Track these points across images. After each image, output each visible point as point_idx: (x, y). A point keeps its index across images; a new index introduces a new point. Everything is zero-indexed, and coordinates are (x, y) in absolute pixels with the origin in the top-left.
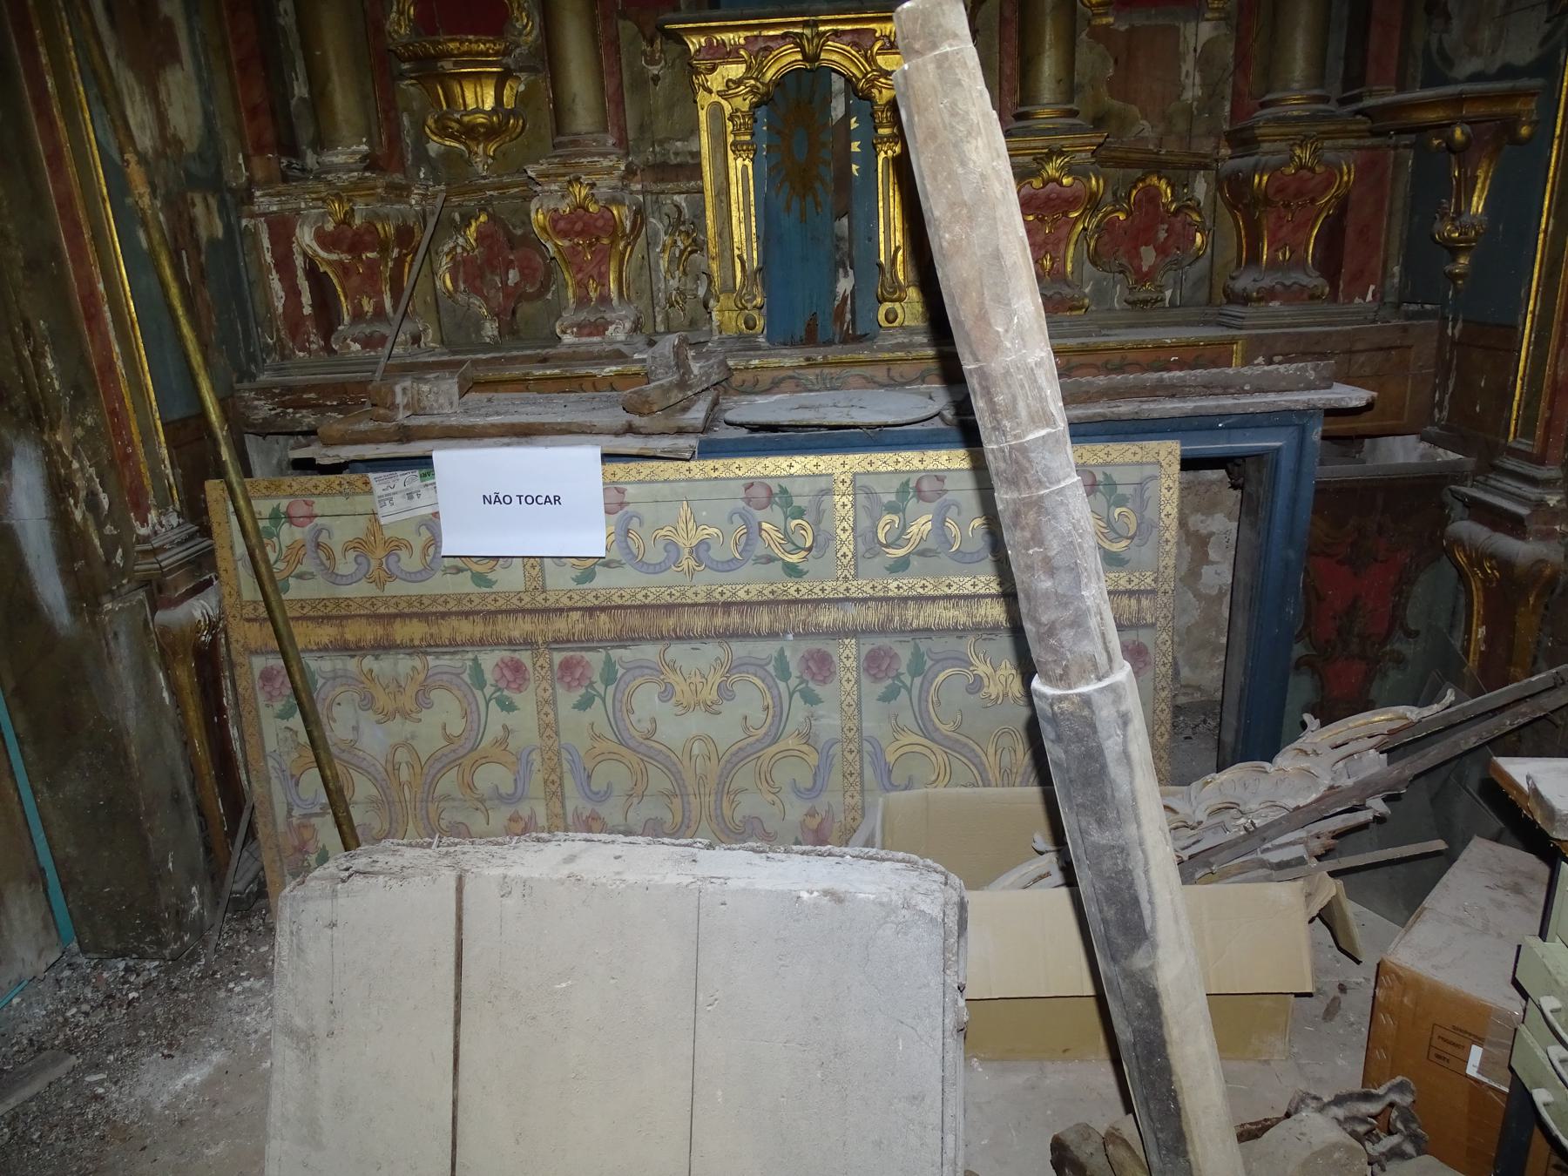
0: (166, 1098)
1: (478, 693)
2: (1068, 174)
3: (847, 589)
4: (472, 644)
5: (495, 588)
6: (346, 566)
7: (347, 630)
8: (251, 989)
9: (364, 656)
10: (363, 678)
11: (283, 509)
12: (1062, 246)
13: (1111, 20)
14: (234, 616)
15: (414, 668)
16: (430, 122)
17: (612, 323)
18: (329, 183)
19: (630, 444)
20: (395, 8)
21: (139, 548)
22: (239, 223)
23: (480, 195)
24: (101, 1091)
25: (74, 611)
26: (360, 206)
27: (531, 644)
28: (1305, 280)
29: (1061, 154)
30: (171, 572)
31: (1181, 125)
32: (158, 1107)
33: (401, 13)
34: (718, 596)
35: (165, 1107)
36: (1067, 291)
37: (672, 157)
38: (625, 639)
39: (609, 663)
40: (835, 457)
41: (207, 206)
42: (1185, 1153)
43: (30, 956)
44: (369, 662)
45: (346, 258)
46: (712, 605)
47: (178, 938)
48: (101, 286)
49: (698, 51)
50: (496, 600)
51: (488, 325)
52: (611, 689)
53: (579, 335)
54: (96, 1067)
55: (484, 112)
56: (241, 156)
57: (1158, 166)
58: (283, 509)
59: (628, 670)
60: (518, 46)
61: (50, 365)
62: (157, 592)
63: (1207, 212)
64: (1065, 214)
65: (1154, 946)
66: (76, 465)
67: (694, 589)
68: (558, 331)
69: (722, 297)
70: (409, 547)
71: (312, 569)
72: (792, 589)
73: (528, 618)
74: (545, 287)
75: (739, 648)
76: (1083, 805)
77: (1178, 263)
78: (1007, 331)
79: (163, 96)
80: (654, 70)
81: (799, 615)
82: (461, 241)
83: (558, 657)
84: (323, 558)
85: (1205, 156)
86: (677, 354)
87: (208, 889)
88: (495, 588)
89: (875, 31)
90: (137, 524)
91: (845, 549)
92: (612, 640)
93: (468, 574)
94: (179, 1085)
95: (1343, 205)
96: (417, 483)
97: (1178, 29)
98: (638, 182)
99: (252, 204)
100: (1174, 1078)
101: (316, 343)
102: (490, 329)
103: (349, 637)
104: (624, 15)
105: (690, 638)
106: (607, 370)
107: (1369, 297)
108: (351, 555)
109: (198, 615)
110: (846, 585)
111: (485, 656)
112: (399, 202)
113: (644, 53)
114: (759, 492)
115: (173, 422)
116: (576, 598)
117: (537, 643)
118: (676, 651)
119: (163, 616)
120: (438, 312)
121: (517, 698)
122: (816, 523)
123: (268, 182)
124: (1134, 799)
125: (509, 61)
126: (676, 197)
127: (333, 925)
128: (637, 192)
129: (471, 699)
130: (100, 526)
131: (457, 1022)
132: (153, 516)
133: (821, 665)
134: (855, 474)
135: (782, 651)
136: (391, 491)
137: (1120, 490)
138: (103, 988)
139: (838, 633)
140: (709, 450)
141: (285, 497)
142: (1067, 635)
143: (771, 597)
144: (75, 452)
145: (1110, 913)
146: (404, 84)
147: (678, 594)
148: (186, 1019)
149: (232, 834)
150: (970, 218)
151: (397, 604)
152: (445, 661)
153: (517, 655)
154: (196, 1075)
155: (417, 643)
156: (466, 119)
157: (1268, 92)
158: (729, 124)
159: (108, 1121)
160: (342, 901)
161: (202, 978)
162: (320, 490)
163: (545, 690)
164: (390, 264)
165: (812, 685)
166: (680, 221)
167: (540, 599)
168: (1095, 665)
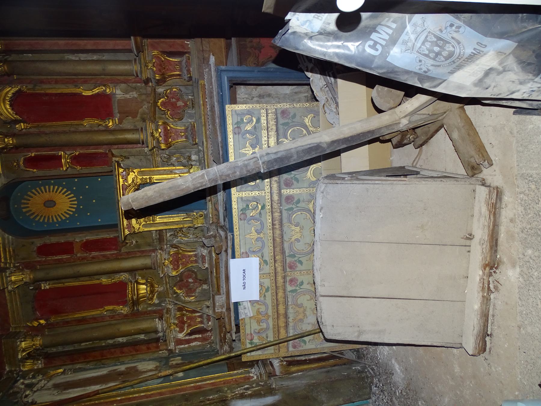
0: (401, 374)
1: (298, 291)
2: (158, 130)
3: (268, 192)
4: (285, 292)
5: (270, 286)
6: (264, 325)
7: (281, 326)
8: (379, 353)
9: (289, 321)
10: (295, 321)
11: (249, 341)
12: (177, 130)
13: (117, 119)
14: (278, 355)
15: (292, 308)
16: (150, 302)
17: (202, 254)
18: (166, 329)
19: (230, 251)
20: (121, 311)
21: (260, 379)
22: (177, 353)
23: (169, 289)
24: (400, 391)
25: (275, 395)
26: (172, 321)
27: (284, 277)
28: (184, 61)
29: (152, 133)
30: (266, 371)
31: (144, 97)
32: (403, 376)
33: (122, 310)
34: (270, 227)
35: (403, 374)
36: (189, 128)
37: (157, 237)
38: (283, 252)
39: (290, 256)
40: (232, 197)
41: (173, 361)
42: (373, 130)
44: (290, 320)
45: (186, 325)
46: (273, 229)
47: (366, 372)
48: (192, 385)
49: (129, 231)
50: (273, 286)
51: (204, 287)
52: (297, 255)
53: (205, 263)
54: (395, 393)
55: (147, 288)
56: (160, 352)
57: (156, 103)
58: (249, 341)
59: (291, 251)
60: (129, 279)
61: (211, 397)
62: (271, 375)
63: (167, 88)
64: (169, 130)
65: (321, 143)
66: (237, 392)
67: (269, 234)
68: (204, 268)
69: (194, 224)
70: (259, 309)
71: (265, 334)
72: (268, 207)
73: (277, 278)
74: (193, 272)
75: (285, 221)
76: (288, 161)
77: (182, 95)
78: (185, 185)
79: (145, 370)
80: (134, 242)
81: (275, 206)
82: (181, 294)
83: (288, 270)
84: (262, 331)
85: (152, 90)
86: (207, 238)
87: (354, 365)
88: (270, 286)
89: (122, 184)
90: (253, 379)
91: (257, 194)
92: (283, 255)
93: (266, 293)
94: (399, 371)
95: (164, 53)
96: (242, 306)
97: (118, 100)
98: (164, 246)
99: (172, 349)
100: (354, 135)
101: (209, 334)
102: (205, 287)
103: (283, 325)
104: (120, 250)
105: (282, 234)
106: (213, 255)
107: (188, 43)
108: (261, 324)
109: (278, 364)
110: (267, 193)
111: (288, 289)
112: (171, 311)
113: (130, 245)
114: (242, 217)
115: (228, 370)
116: (272, 265)
117: (284, 275)
118: (286, 238)
119: (278, 373)
120: (201, 301)
121: (299, 281)
122: (250, 201)
123: (166, 345)
124: (286, 150)
125: (133, 281)
126: (168, 236)
127: (333, 326)
128: (167, 246)
129: (300, 293)
130: (253, 387)
131: (355, 297)
132: (251, 375)
133: (289, 199)
134: (237, 191)
135: (285, 210)
136: (244, 313)
137: (239, 120)
138: (380, 393)
139: (280, 194)
140: (231, 230)
141: (246, 341)
142: (249, 168)
143: (270, 213)
144: (234, 393)
145: (314, 153)
146: (140, 309)
147: (270, 238)
148: (385, 370)
149: (340, 358)
150: (163, 194)
151: (274, 312)
152: (290, 300)
153: (288, 281)
154: (397, 367)
155: (285, 307)
156: (149, 293)
157: (134, 75)
158: (148, 222)
160: (327, 323)
161: (377, 366)
162: (244, 332)
163: (297, 273)
164: (187, 313)
165: (294, 201)
166: (174, 235)
167: (272, 275)
168: (255, 161)
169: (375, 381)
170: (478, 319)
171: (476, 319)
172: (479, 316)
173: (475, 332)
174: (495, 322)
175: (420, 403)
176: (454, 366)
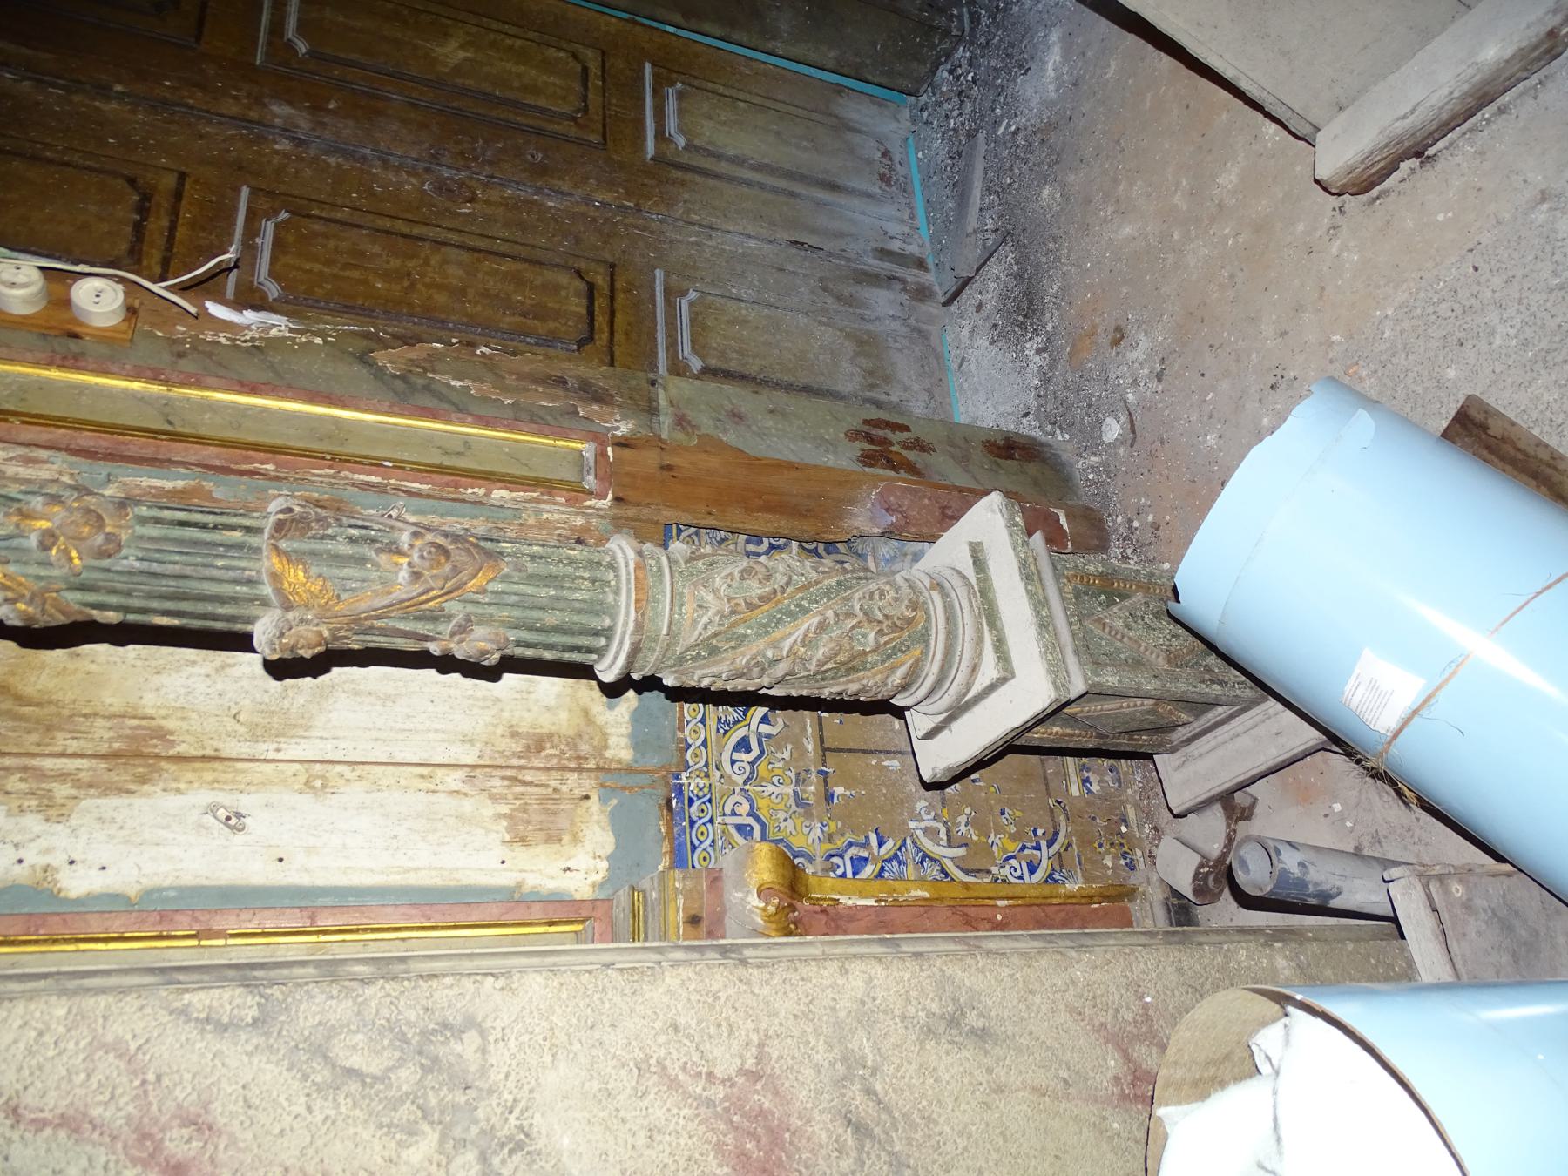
0: (1052, 87)
24: (1013, 128)
32: (1053, 95)
35: (1057, 90)
43: (893, 126)
54: (997, 123)
94: (1051, 73)
148: (1012, 45)
154: (1054, 57)
159: (1035, 133)
161: (994, 19)
169: (957, 56)
170: (1451, 93)
171: (1445, 91)
172: (1466, 87)
173: (1400, 127)
174: (1485, 133)
175: (1046, 192)
176: (1229, 165)
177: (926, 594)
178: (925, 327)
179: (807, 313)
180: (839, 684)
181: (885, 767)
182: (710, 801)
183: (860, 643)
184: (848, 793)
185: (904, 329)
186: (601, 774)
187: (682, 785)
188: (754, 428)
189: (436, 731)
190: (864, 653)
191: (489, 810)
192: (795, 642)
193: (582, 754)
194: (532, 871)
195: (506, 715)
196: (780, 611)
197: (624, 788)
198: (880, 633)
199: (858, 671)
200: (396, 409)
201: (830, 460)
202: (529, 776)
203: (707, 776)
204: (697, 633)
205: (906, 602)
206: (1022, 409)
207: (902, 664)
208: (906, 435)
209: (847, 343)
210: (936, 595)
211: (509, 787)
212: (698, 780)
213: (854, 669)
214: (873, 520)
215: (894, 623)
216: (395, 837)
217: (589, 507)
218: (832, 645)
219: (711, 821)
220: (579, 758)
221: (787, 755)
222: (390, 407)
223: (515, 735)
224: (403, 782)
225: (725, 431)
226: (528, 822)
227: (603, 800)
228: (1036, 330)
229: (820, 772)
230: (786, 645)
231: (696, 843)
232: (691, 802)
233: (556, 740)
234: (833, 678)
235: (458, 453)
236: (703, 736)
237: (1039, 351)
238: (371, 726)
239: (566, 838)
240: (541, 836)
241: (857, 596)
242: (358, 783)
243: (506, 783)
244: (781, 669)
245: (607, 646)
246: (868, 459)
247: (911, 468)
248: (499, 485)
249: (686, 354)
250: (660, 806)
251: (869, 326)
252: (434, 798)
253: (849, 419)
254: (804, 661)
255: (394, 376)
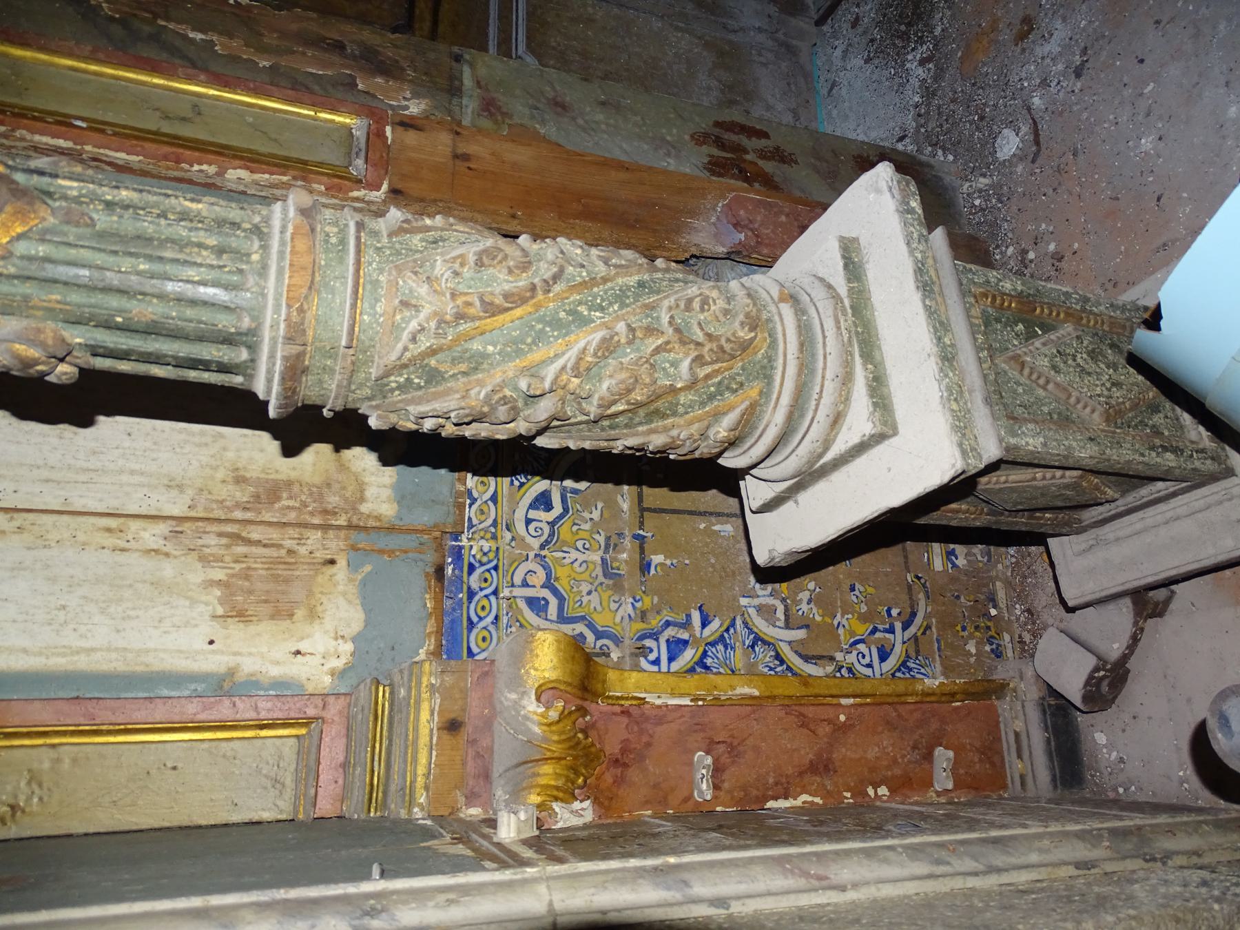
177: (773, 308)
178: (794, 42)
179: (662, 17)
180: (636, 434)
181: (715, 532)
182: (496, 568)
183: (667, 375)
184: (668, 562)
185: (770, 43)
186: (353, 534)
187: (461, 548)
188: (580, 121)
189: (132, 472)
190: (673, 390)
191: (197, 575)
192: (563, 368)
193: (330, 507)
194: (250, 654)
195: (230, 455)
196: (540, 320)
197: (381, 552)
198: (699, 360)
199: (664, 416)
200: (101, 56)
201: (671, 164)
202: (255, 534)
203: (494, 537)
204: (400, 346)
205: (741, 317)
206: (898, 132)
207: (731, 408)
208: (763, 142)
209: (705, 53)
210: (787, 310)
211: (228, 546)
212: (483, 542)
213: (658, 414)
214: (716, 236)
215: (721, 348)
216: (64, 607)
217: (357, 199)
218: (624, 375)
219: (495, 593)
220: (325, 512)
221: (596, 515)
222: (94, 51)
223: (240, 480)
224: (81, 537)
225: (543, 122)
226: (250, 592)
227: (352, 566)
228: (921, 38)
229: (636, 537)
230: (550, 372)
231: (475, 619)
232: (472, 568)
233: (296, 488)
234: (627, 426)
235: (184, 119)
236: (492, 489)
237: (922, 62)
238: (40, 462)
239: (300, 613)
240: (265, 609)
241: (666, 303)
242: (16, 537)
243: (224, 541)
244: (543, 410)
245: (253, 361)
246: (716, 167)
247: (769, 183)
248: (237, 162)
249: (520, 52)
250: (427, 575)
251: (732, 37)
252: (121, 558)
253: (697, 119)
254: (579, 398)
255: (112, 19)
